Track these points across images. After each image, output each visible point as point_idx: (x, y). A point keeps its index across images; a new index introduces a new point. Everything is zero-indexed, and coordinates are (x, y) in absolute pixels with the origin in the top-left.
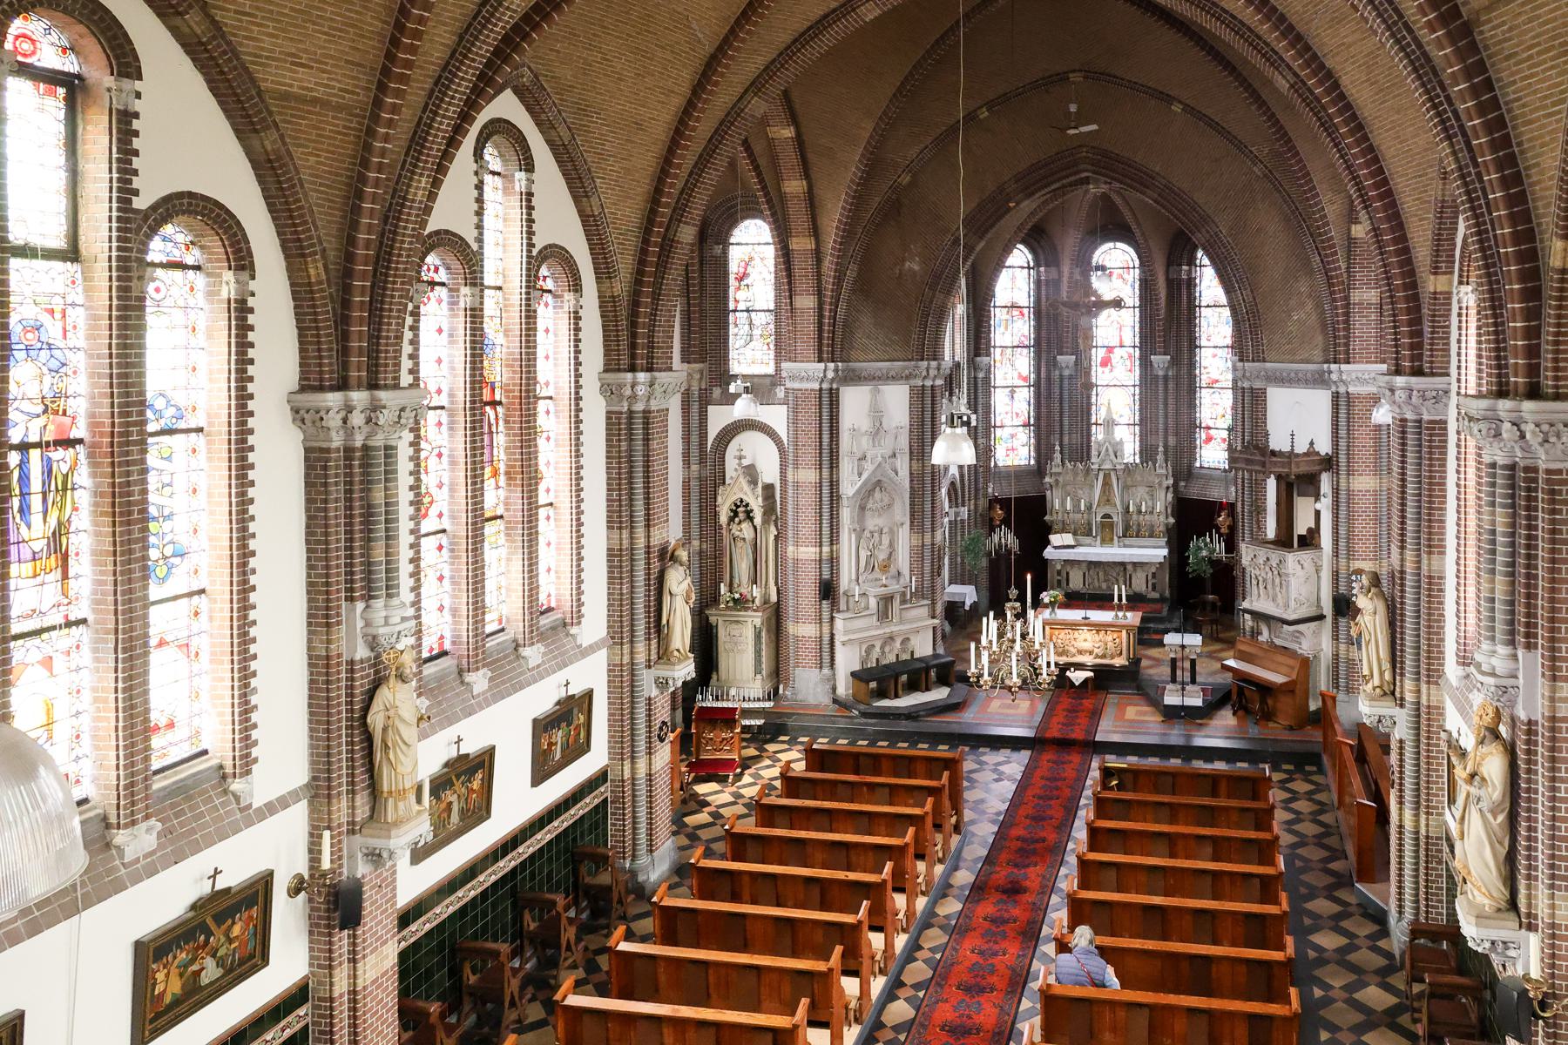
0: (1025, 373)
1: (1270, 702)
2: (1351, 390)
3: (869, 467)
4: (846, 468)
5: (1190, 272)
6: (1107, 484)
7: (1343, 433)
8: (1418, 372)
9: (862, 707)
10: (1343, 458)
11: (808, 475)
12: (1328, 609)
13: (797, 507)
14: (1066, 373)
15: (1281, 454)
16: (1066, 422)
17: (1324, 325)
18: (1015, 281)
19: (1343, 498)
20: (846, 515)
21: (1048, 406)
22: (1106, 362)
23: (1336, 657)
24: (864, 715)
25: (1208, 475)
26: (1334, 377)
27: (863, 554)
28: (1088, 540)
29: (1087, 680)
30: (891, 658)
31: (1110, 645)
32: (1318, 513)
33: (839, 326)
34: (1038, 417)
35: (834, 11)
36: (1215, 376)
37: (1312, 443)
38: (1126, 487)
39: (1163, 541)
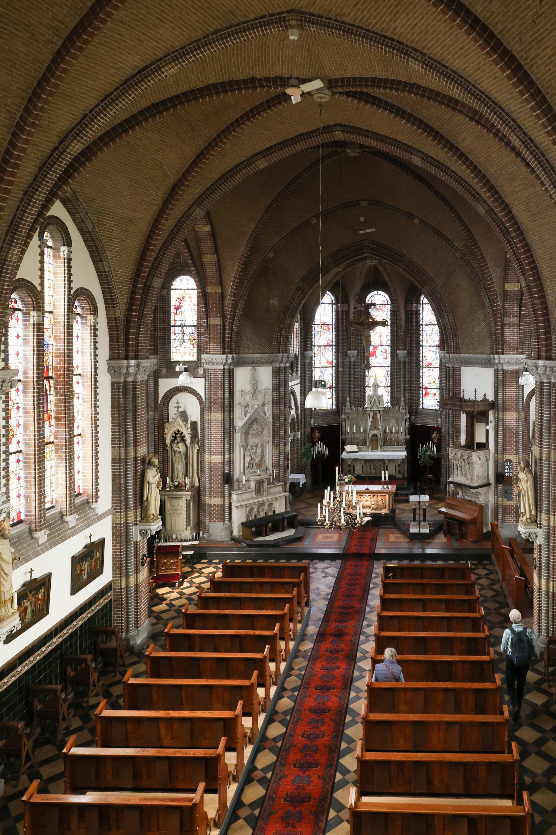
0: (330, 360)
1: (464, 529)
2: (505, 368)
3: (250, 411)
4: (238, 412)
5: (417, 307)
6: (375, 418)
7: (500, 390)
8: (549, 358)
9: (248, 542)
10: (500, 403)
11: (217, 416)
12: (492, 480)
13: (210, 434)
14: (353, 360)
15: (469, 401)
16: (352, 386)
17: (491, 335)
18: (325, 312)
19: (500, 423)
20: (238, 437)
21: (343, 377)
23: (497, 504)
24: (249, 546)
25: (428, 412)
26: (496, 361)
27: (247, 459)
28: (365, 448)
29: (368, 521)
30: (262, 515)
32: (487, 431)
33: (234, 334)
34: (337, 383)
35: (243, 162)
36: (430, 361)
37: (485, 395)
38: (384, 420)
39: (404, 448)
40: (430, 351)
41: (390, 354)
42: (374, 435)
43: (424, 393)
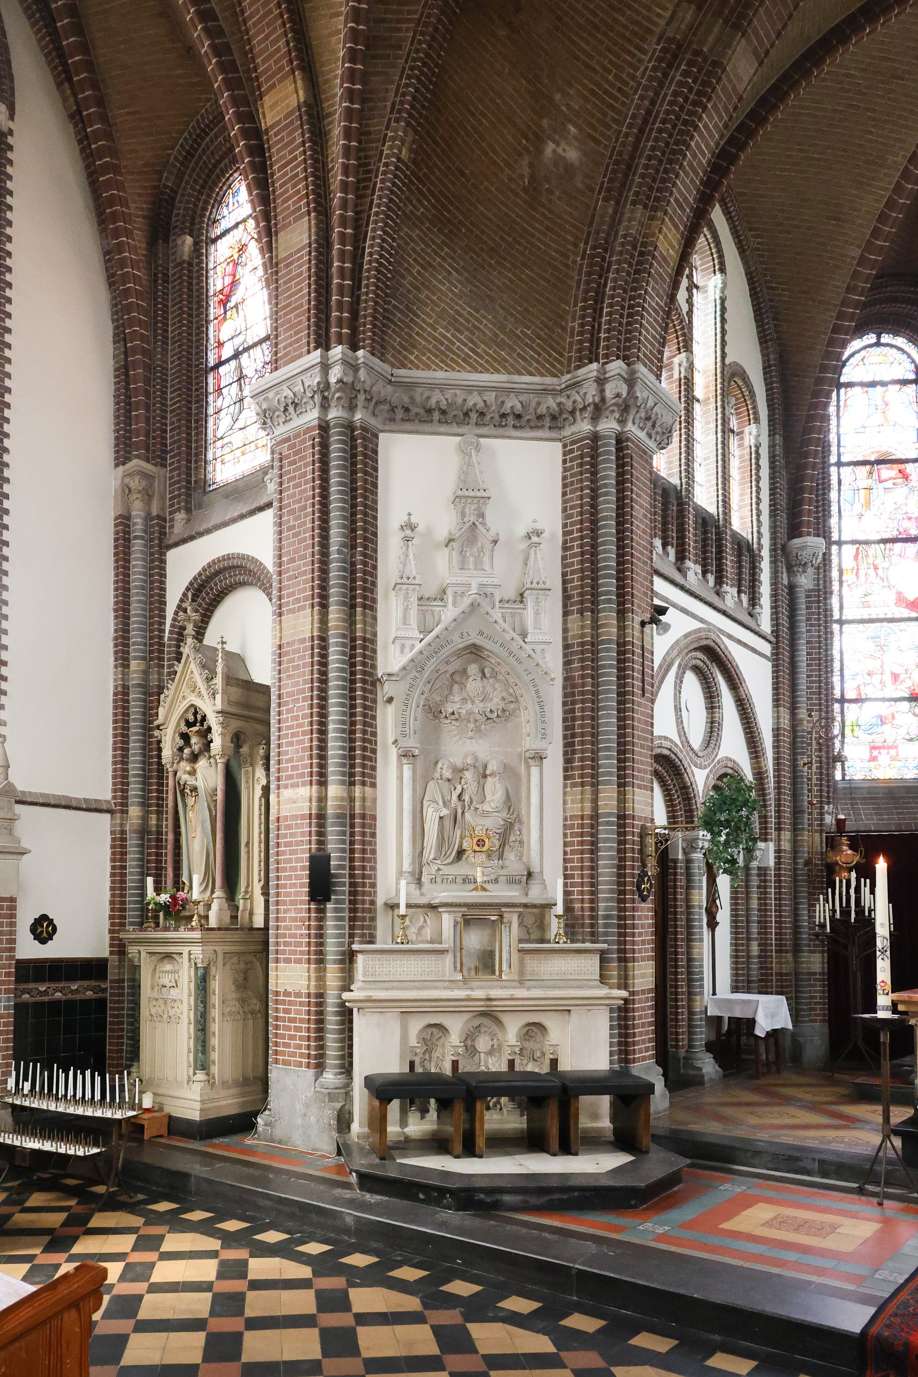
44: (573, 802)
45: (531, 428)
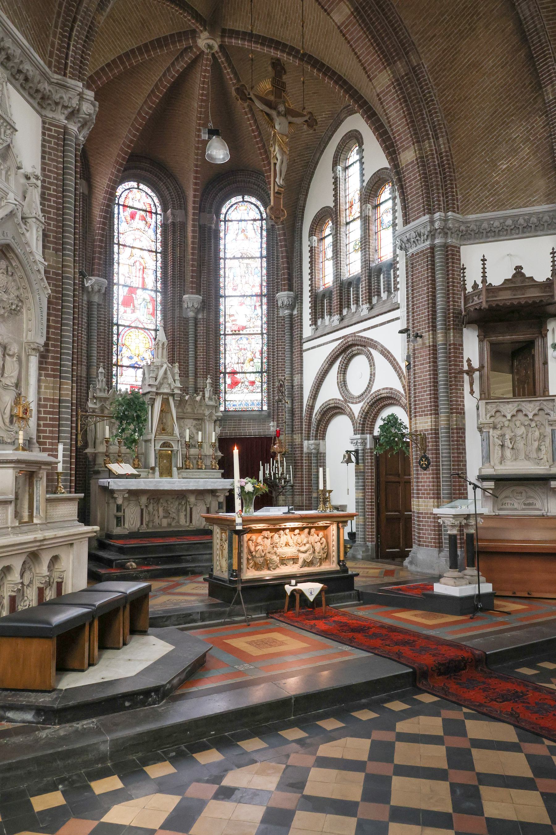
22: (128, 302)
31: (318, 547)
36: (241, 321)
40: (242, 304)
41: (159, 308)
42: (166, 445)
43: (229, 381)
44: (46, 388)
45: (29, 93)
